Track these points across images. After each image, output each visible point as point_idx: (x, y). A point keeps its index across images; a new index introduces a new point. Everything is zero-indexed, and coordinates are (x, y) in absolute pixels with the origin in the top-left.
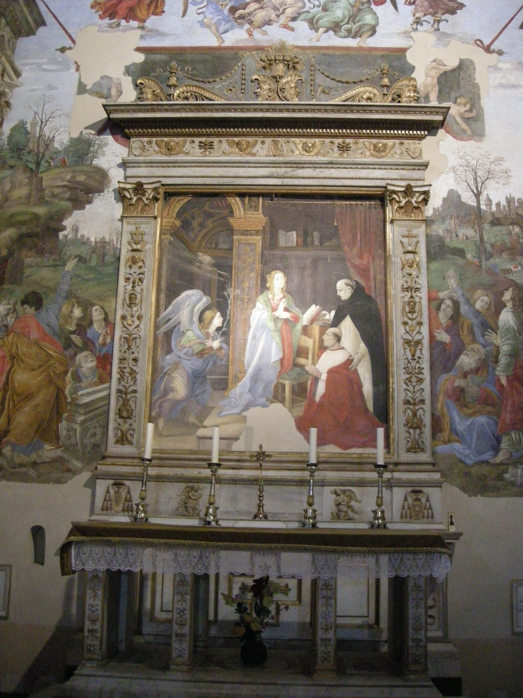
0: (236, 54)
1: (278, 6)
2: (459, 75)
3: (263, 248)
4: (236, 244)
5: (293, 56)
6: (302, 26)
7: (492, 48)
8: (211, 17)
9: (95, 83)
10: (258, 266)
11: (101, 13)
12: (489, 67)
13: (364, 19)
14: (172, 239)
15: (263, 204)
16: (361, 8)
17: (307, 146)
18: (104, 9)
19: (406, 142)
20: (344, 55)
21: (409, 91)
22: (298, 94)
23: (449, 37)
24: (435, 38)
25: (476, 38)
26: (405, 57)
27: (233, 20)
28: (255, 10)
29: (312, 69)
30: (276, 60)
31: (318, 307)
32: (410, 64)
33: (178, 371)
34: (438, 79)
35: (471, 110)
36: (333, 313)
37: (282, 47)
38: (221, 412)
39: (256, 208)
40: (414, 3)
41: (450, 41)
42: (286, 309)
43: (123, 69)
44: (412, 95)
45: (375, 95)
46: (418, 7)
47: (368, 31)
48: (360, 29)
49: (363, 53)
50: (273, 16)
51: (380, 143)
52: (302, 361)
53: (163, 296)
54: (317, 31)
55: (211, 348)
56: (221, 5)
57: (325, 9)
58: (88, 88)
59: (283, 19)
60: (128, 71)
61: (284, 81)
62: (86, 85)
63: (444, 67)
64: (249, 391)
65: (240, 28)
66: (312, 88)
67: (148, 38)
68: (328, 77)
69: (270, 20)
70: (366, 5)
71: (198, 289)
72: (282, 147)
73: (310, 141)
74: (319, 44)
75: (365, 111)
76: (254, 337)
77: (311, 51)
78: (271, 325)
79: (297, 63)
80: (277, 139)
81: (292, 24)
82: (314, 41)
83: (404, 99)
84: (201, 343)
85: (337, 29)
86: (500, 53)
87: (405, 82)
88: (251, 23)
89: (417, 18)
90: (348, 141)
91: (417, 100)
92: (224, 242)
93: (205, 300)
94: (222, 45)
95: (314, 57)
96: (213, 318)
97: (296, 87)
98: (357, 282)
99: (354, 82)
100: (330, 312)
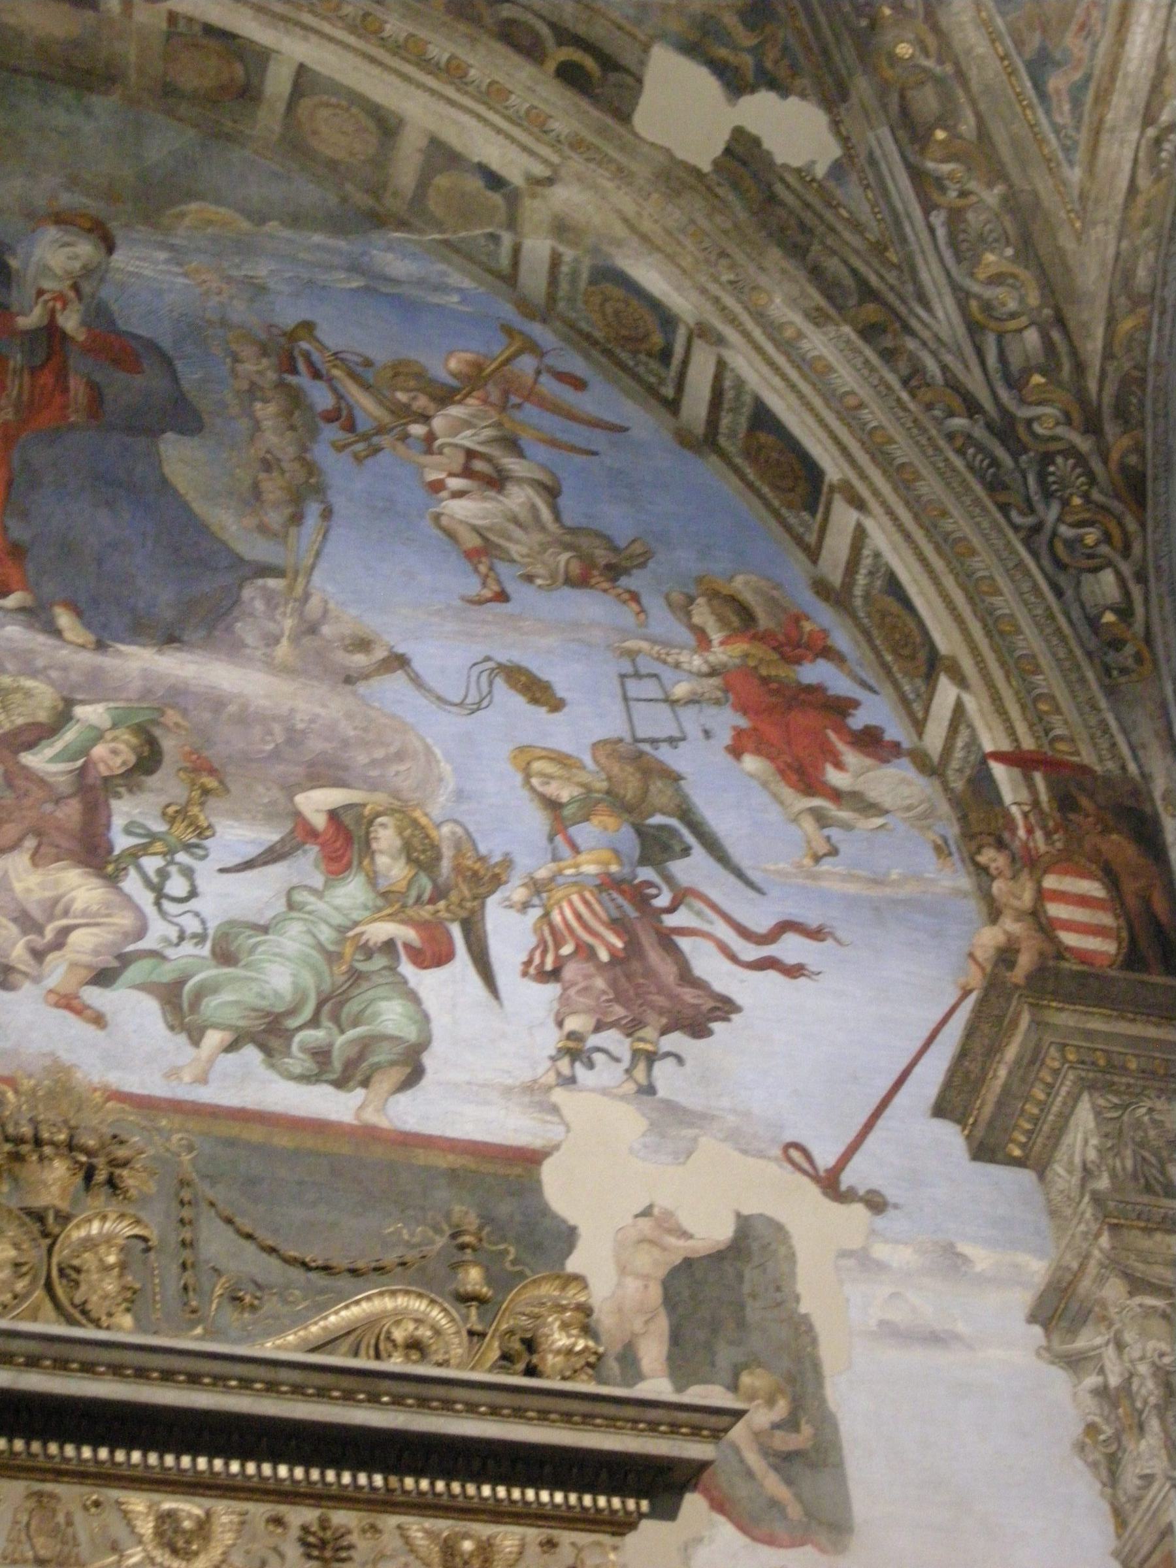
1: (37, 913)
2: (740, 1277)
5: (107, 1131)
7: (847, 1179)
12: (844, 1254)
13: (376, 1015)
17: (177, 1530)
19: (566, 1537)
21: (565, 1326)
22: (132, 1299)
23: (691, 1125)
24: (642, 1124)
25: (789, 1137)
26: (536, 1188)
29: (186, 1194)
30: (38, 1142)
32: (555, 1217)
34: (667, 1284)
35: (791, 1424)
40: (554, 975)
41: (695, 1139)
44: (581, 1345)
45: (437, 1332)
46: (572, 992)
47: (393, 1063)
48: (361, 1056)
51: (466, 1536)
54: (196, 1041)
59: (57, 971)
61: (78, 1234)
63: (681, 1243)
66: (188, 1276)
68: (249, 1237)
70: (380, 961)
72: (69, 1523)
73: (189, 1508)
74: (207, 1095)
75: (423, 1403)
77: (178, 1119)
79: (125, 1164)
80: (49, 1487)
81: (94, 996)
82: (187, 1078)
83: (550, 1359)
85: (275, 1043)
86: (876, 1203)
87: (548, 1290)
89: (571, 1036)
90: (341, 1517)
91: (594, 1365)
95: (190, 1148)
97: (123, 1266)
99: (354, 1272)
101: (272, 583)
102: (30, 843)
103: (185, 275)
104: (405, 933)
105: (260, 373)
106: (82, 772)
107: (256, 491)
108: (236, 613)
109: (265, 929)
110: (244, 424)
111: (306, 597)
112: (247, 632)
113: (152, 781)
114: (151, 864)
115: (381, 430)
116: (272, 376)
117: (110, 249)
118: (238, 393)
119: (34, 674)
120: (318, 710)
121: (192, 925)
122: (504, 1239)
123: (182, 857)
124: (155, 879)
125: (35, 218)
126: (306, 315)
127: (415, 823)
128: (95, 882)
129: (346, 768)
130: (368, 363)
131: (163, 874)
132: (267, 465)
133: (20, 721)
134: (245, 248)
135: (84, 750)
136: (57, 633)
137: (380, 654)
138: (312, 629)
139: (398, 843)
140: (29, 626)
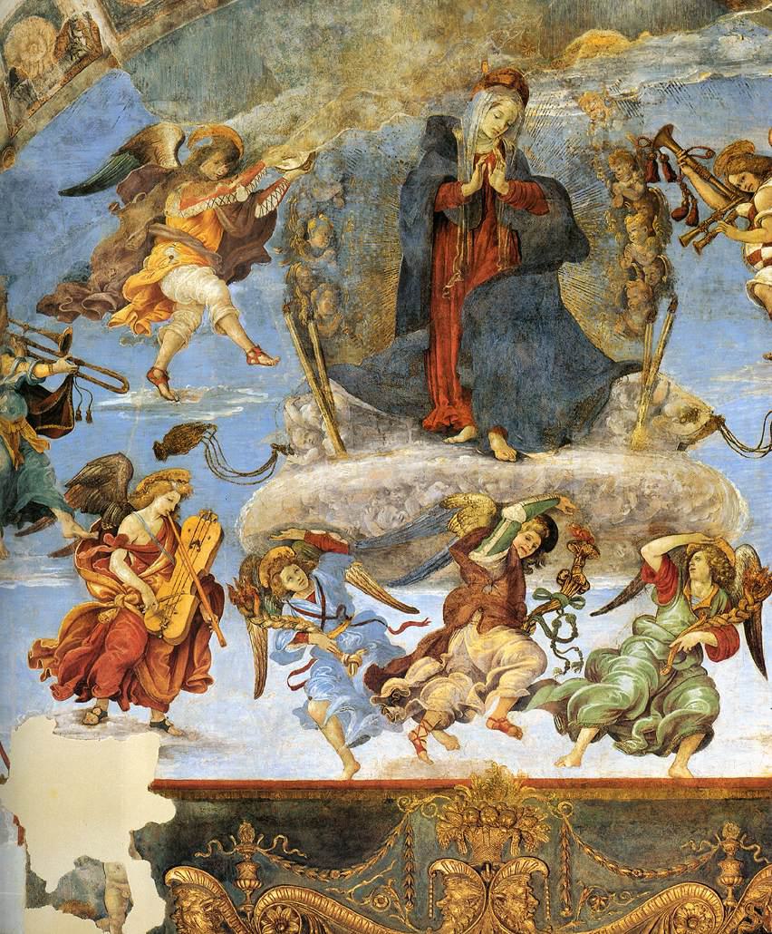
0: (390, 801)
1: (481, 666)
6: (537, 720)
8: (326, 701)
9: (65, 877)
11: (54, 680)
13: (687, 699)
16: (676, 667)
18: (61, 669)
20: (641, 802)
27: (377, 707)
28: (428, 679)
37: (494, 784)
43: (127, 841)
47: (693, 733)
48: (674, 731)
49: (681, 794)
50: (471, 698)
54: (574, 739)
56: (347, 663)
57: (593, 676)
58: (50, 889)
59: (494, 705)
60: (141, 844)
62: (45, 883)
65: (394, 729)
67: (177, 755)
69: (465, 708)
70: (690, 661)
81: (516, 718)
82: (568, 764)
85: (622, 731)
88: (420, 715)
94: (356, 777)
101: (634, 378)
102: (477, 618)
103: (578, 108)
104: (710, 638)
105: (630, 187)
106: (508, 558)
107: (624, 298)
108: (607, 409)
109: (618, 652)
110: (614, 243)
111: (656, 382)
112: (614, 423)
113: (551, 556)
114: (549, 618)
115: (715, 218)
116: (639, 187)
117: (525, 101)
118: (612, 210)
119: (477, 490)
120: (660, 476)
121: (573, 657)
122: (754, 842)
123: (569, 609)
124: (552, 629)
125: (470, 86)
126: (666, 121)
127: (720, 553)
128: (517, 637)
129: (675, 519)
130: (710, 153)
131: (557, 624)
132: (632, 274)
133: (469, 529)
134: (622, 67)
135: (508, 542)
136: (491, 454)
137: (704, 419)
138: (659, 411)
139: (707, 570)
140: (474, 453)
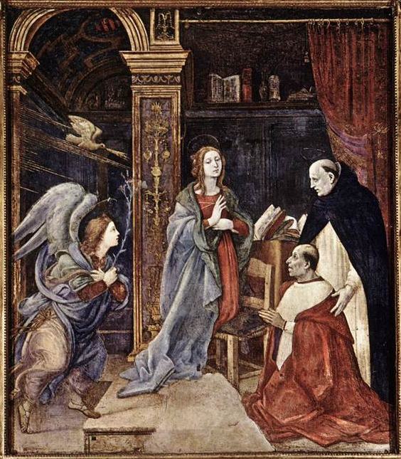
3: (184, 107)
4: (136, 100)
10: (177, 139)
14: (25, 92)
15: (182, 25)
31: (279, 209)
33: (48, 322)
36: (304, 218)
38: (122, 390)
39: (171, 32)
42: (225, 214)
52: (254, 301)
53: (16, 195)
55: (102, 282)
64: (168, 354)
71: (75, 182)
76: (173, 262)
78: (201, 243)
84: (83, 276)
92: (115, 97)
93: (89, 199)
96: (102, 232)
98: (342, 163)
100: (298, 218)
